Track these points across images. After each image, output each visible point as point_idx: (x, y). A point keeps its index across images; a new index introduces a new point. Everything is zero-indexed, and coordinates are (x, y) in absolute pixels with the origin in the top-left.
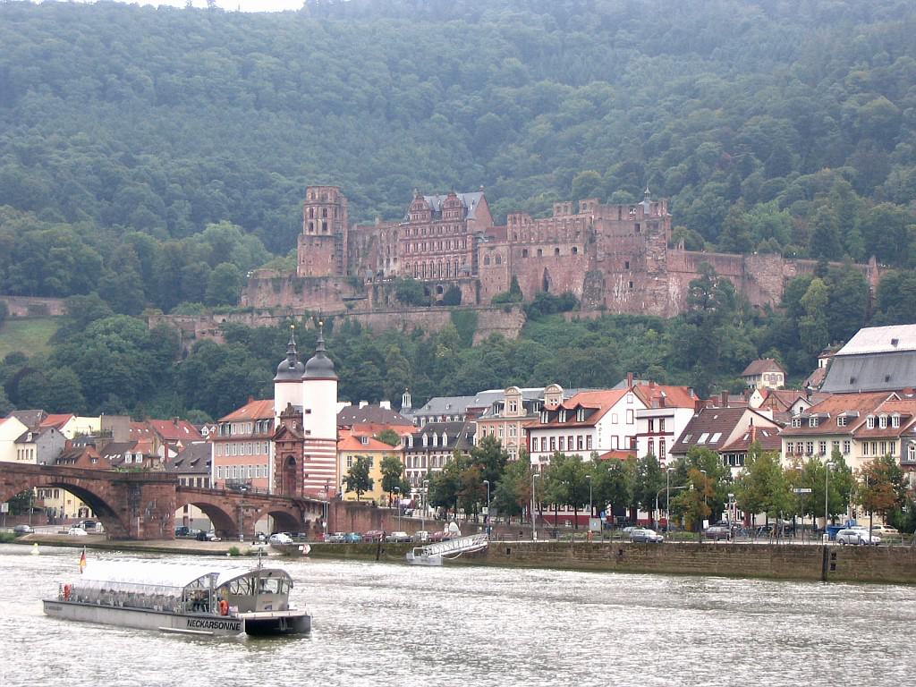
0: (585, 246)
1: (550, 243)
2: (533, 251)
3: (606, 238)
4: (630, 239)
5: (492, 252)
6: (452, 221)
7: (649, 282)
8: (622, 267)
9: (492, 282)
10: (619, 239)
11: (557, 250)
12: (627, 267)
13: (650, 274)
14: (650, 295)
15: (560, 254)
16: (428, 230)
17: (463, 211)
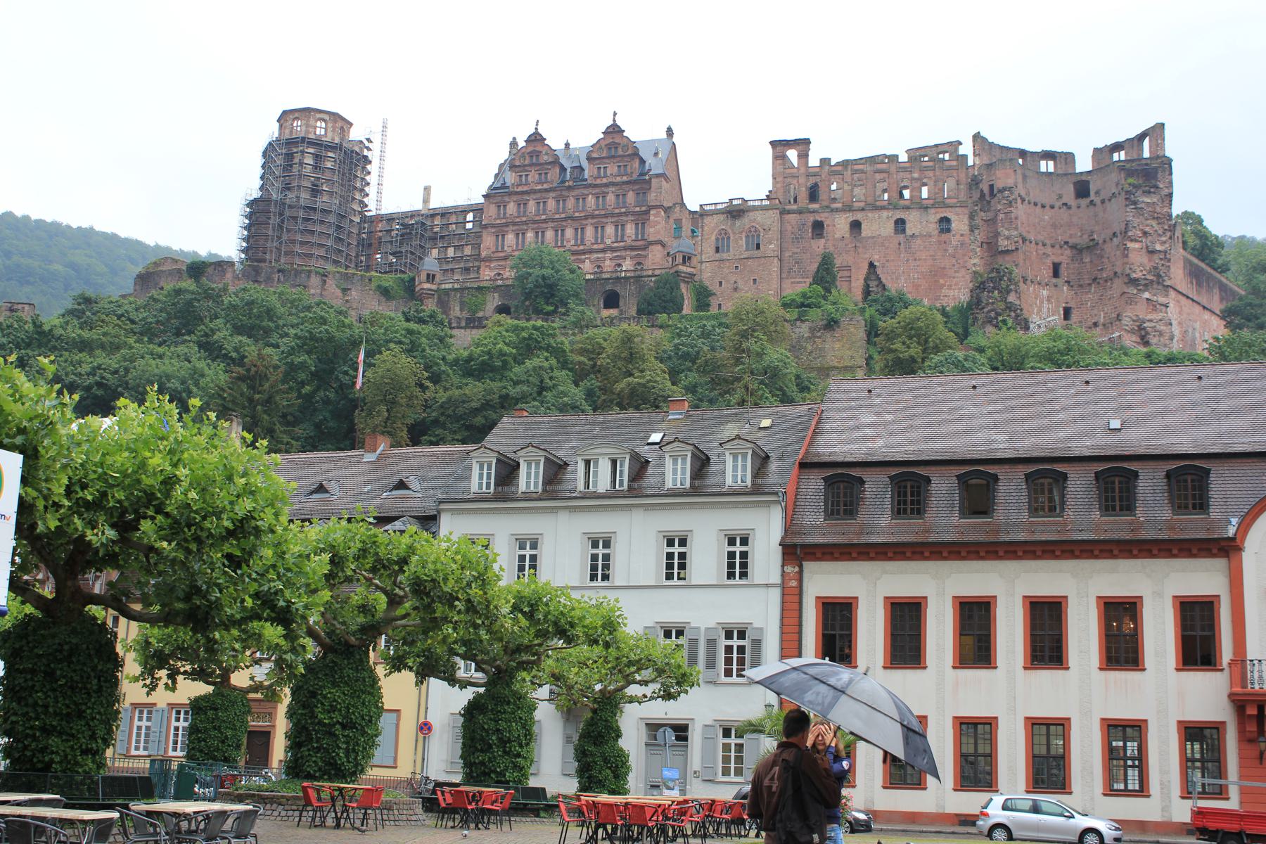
0: (971, 217)
1: (883, 208)
2: (839, 225)
3: (1019, 201)
4: (1064, 215)
5: (738, 223)
6: (614, 184)
7: (1131, 301)
8: (1047, 272)
9: (736, 289)
10: (1038, 209)
11: (900, 224)
12: (1056, 274)
13: (1134, 282)
14: (1131, 332)
15: (909, 232)
16: (551, 204)
17: (636, 164)
